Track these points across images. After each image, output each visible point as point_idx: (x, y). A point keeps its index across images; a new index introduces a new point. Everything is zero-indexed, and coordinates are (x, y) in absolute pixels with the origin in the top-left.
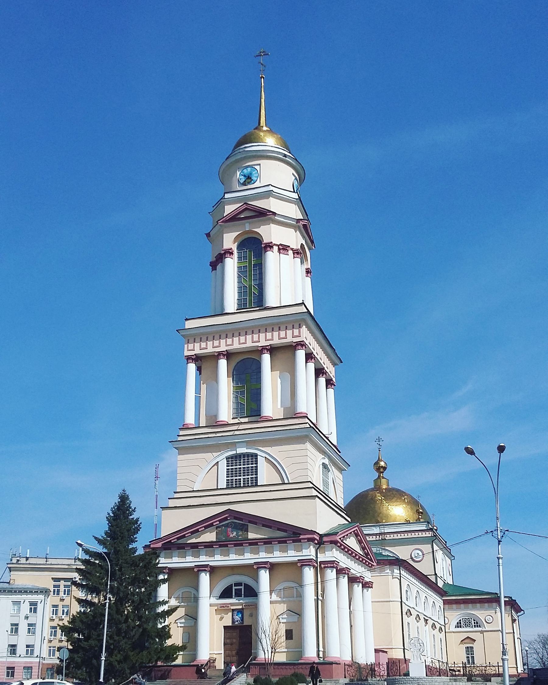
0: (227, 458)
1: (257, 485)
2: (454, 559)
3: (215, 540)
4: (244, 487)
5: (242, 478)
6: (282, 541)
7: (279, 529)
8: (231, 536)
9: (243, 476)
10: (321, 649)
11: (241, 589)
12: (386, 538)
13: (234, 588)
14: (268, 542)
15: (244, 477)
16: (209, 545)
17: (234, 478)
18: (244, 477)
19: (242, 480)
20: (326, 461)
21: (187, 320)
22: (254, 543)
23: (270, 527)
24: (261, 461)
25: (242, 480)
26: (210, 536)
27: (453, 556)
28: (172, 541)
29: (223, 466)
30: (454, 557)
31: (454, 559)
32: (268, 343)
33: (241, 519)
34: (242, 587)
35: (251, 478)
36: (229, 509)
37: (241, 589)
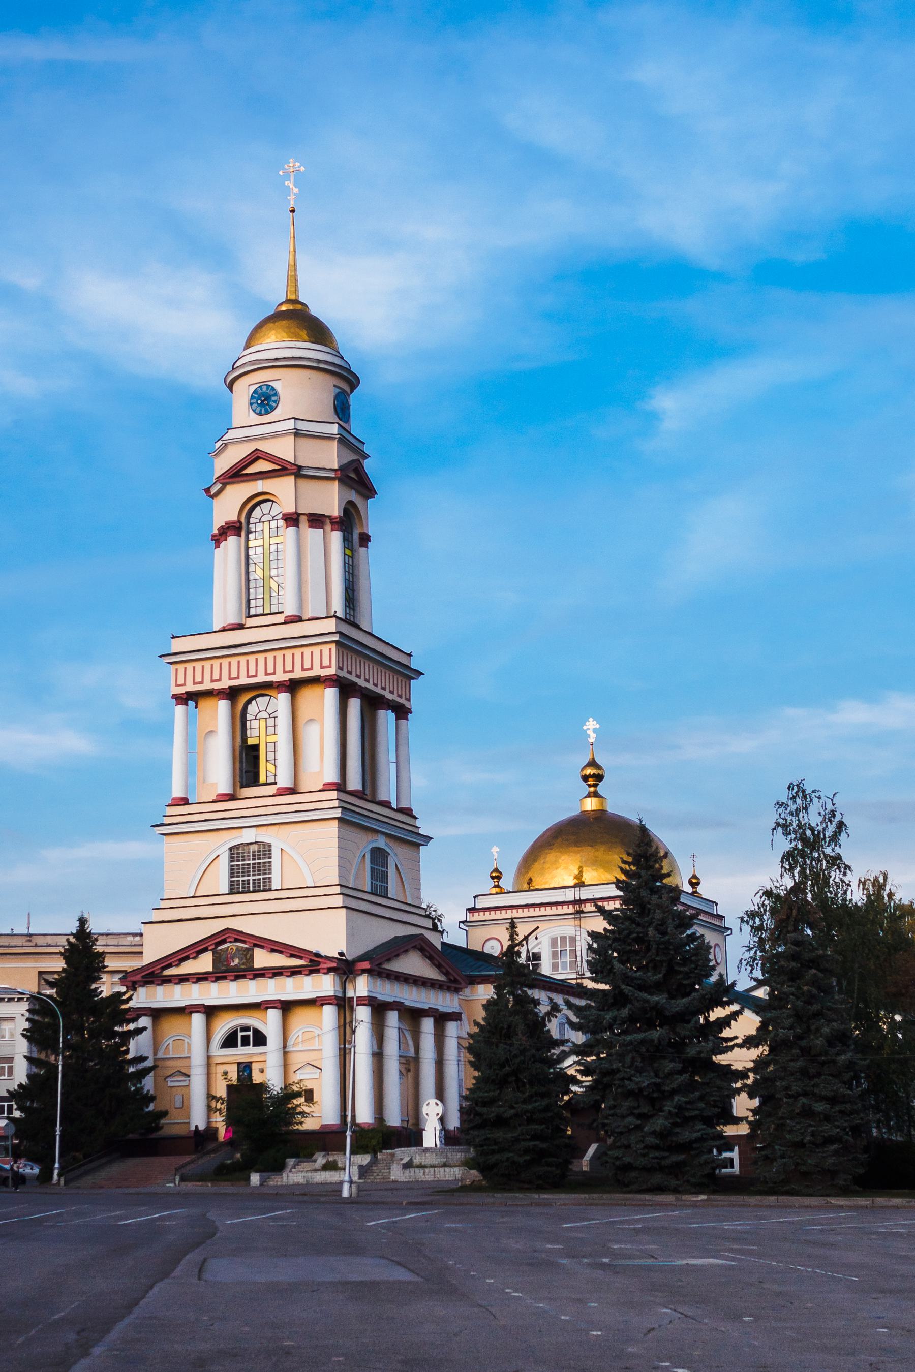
0: (231, 849)
1: (270, 890)
2: (731, 934)
3: (210, 969)
4: (254, 892)
5: (251, 878)
6: (294, 972)
7: (292, 956)
8: (232, 964)
9: (254, 875)
10: (349, 1113)
11: (249, 1036)
12: (585, 910)
13: (240, 1034)
14: (277, 972)
15: (254, 877)
16: (200, 978)
17: (241, 879)
18: (254, 877)
19: (251, 882)
20: (381, 842)
21: (173, 637)
22: (261, 974)
23: (281, 952)
24: (275, 853)
25: (251, 882)
26: (205, 963)
27: (729, 929)
28: (156, 972)
29: (224, 864)
30: (731, 929)
31: (731, 934)
32: (286, 677)
33: (244, 942)
34: (251, 1033)
35: (264, 879)
36: (227, 929)
37: (249, 1035)
